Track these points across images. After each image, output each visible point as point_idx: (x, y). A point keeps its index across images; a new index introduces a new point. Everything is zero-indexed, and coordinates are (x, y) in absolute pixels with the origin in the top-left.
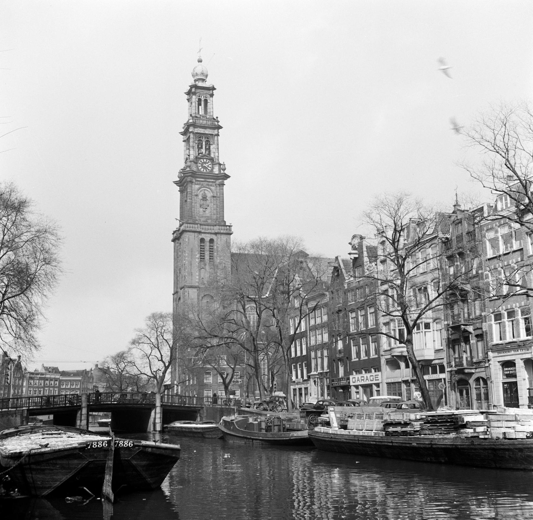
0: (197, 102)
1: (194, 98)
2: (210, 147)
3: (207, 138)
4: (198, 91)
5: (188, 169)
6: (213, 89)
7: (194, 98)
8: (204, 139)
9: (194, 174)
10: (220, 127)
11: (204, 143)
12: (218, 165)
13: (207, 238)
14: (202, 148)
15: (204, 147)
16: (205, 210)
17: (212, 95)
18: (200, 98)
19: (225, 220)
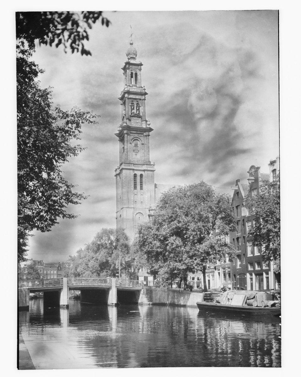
0: (130, 75)
1: (129, 72)
2: (139, 108)
3: (138, 102)
4: (131, 66)
5: (125, 124)
6: (141, 65)
7: (129, 72)
8: (135, 102)
9: (129, 128)
10: (146, 94)
11: (135, 106)
12: (145, 121)
13: (139, 173)
14: (133, 109)
15: (135, 108)
16: (136, 154)
17: (140, 70)
18: (132, 71)
19: (150, 160)
